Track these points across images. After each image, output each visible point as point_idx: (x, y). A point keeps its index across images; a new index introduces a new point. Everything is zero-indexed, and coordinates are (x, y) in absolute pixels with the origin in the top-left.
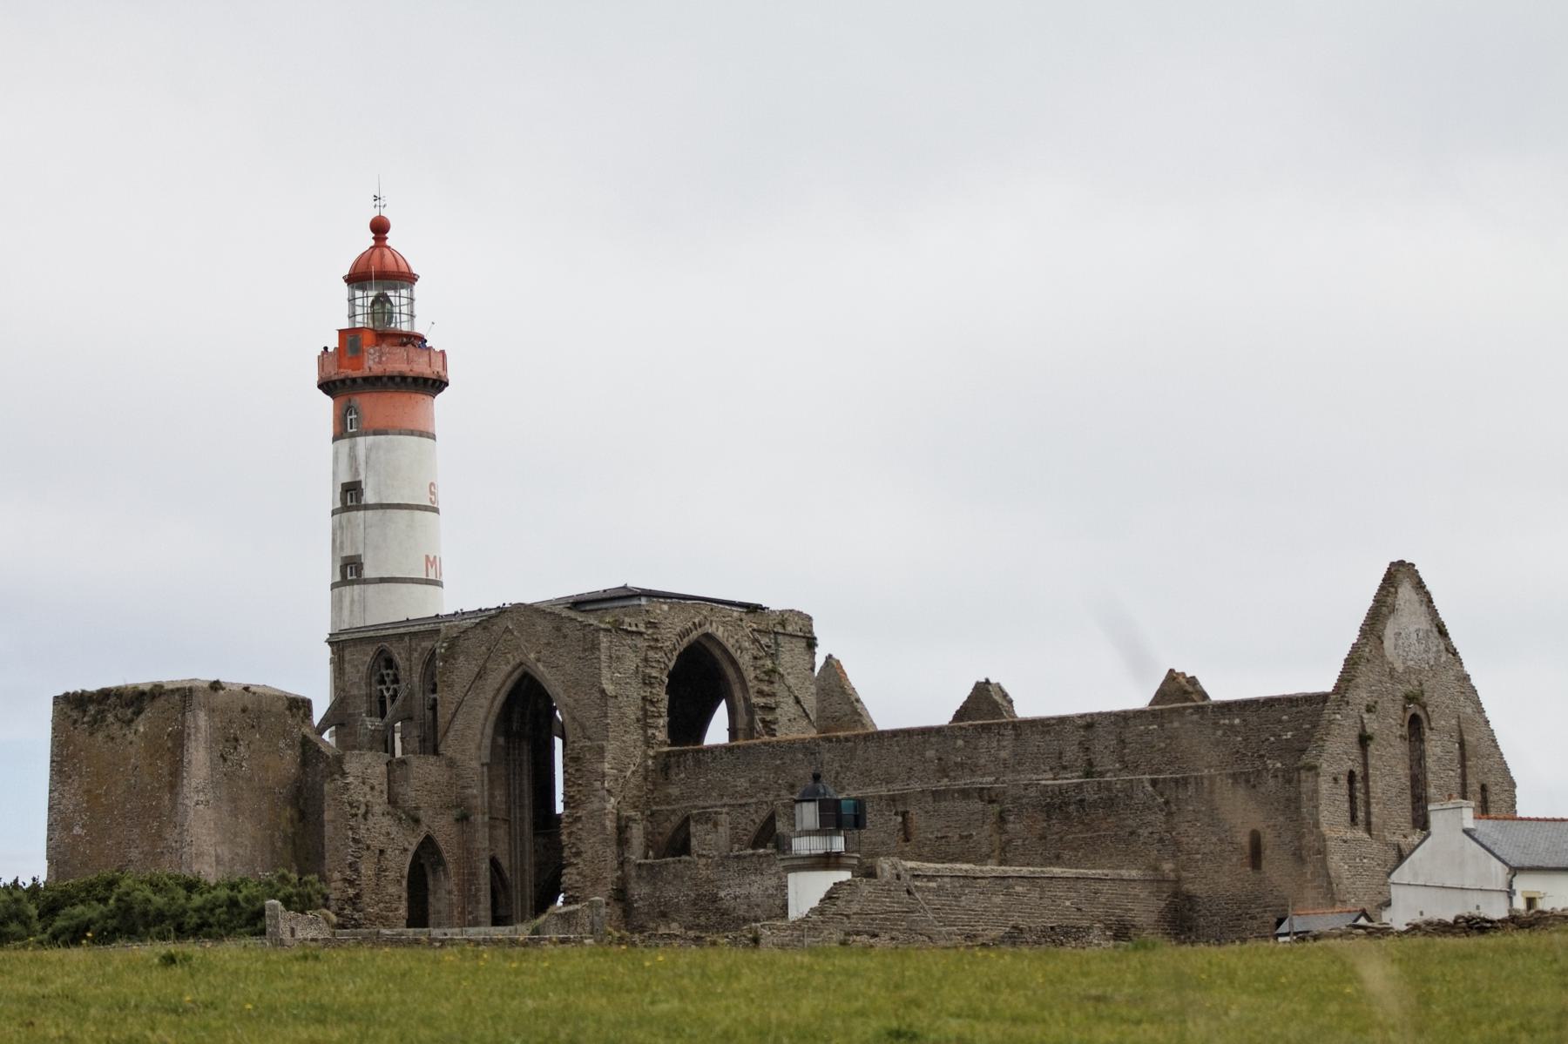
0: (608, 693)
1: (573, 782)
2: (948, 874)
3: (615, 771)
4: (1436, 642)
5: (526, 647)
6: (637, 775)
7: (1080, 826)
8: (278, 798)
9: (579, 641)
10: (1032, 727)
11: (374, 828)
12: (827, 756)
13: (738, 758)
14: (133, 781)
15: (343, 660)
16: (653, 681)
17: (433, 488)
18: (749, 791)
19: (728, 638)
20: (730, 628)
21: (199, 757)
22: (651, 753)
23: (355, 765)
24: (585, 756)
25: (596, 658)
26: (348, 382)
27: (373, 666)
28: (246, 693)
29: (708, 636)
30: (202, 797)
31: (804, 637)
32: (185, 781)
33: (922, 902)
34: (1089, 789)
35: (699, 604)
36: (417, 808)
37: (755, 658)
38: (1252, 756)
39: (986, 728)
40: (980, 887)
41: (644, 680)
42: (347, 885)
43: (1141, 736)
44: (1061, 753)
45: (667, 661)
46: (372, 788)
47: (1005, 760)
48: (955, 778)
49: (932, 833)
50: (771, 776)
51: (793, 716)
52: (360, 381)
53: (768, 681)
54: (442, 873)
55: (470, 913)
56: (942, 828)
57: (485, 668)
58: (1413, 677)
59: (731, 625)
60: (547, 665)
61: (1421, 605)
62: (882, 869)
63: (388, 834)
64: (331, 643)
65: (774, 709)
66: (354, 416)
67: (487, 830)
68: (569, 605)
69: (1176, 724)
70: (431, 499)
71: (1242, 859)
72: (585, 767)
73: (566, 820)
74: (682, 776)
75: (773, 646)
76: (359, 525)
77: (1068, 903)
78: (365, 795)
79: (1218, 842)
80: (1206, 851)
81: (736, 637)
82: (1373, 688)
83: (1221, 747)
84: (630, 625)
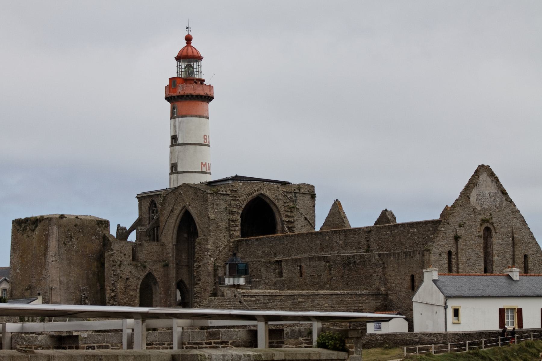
0: (211, 218)
1: (199, 252)
2: (262, 294)
3: (214, 248)
4: (500, 197)
5: (186, 200)
6: (226, 249)
7: (355, 272)
8: (91, 259)
9: (202, 198)
10: (350, 232)
11: (124, 270)
12: (286, 243)
13: (259, 243)
14: (34, 253)
15: (141, 204)
16: (233, 213)
17: (205, 137)
18: (262, 256)
19: (271, 195)
20: (272, 191)
21: (53, 244)
22: (232, 240)
23: (116, 246)
24: (202, 242)
25: (207, 204)
26: (172, 98)
27: (150, 206)
28: (76, 219)
29: (261, 194)
30: (54, 259)
31: (310, 194)
32: (48, 253)
33: (247, 306)
34: (357, 257)
35: (257, 182)
36: (145, 262)
37: (285, 203)
38: (420, 244)
39: (336, 232)
40: (279, 300)
41: (229, 212)
42: (111, 292)
43: (385, 236)
44: (359, 242)
45: (241, 205)
46: (125, 255)
47: (341, 245)
48: (326, 252)
49: (309, 274)
50: (269, 250)
51: (304, 225)
52: (176, 97)
53: (290, 211)
54: (157, 286)
55: (169, 301)
56: (312, 272)
57: (174, 208)
58: (487, 212)
59: (273, 190)
60: (192, 207)
61: (492, 182)
62: (226, 293)
63: (131, 272)
64: (138, 198)
65: (293, 222)
66: (175, 111)
67: (175, 270)
68: (207, 184)
69: (396, 231)
70: (204, 141)
71: (408, 286)
72: (202, 246)
73: (196, 267)
74: (242, 249)
75: (294, 198)
76: (176, 151)
77: (326, 305)
78: (121, 257)
79: (400, 279)
80: (396, 283)
81: (275, 195)
82: (463, 217)
83: (410, 240)
84: (223, 191)
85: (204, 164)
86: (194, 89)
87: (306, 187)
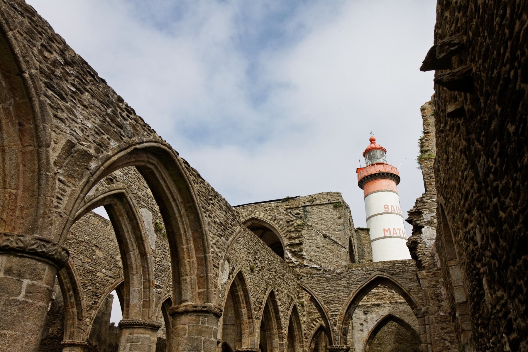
20: (269, 212)
37: (288, 222)
85: (387, 230)
86: (367, 171)
87: (325, 196)
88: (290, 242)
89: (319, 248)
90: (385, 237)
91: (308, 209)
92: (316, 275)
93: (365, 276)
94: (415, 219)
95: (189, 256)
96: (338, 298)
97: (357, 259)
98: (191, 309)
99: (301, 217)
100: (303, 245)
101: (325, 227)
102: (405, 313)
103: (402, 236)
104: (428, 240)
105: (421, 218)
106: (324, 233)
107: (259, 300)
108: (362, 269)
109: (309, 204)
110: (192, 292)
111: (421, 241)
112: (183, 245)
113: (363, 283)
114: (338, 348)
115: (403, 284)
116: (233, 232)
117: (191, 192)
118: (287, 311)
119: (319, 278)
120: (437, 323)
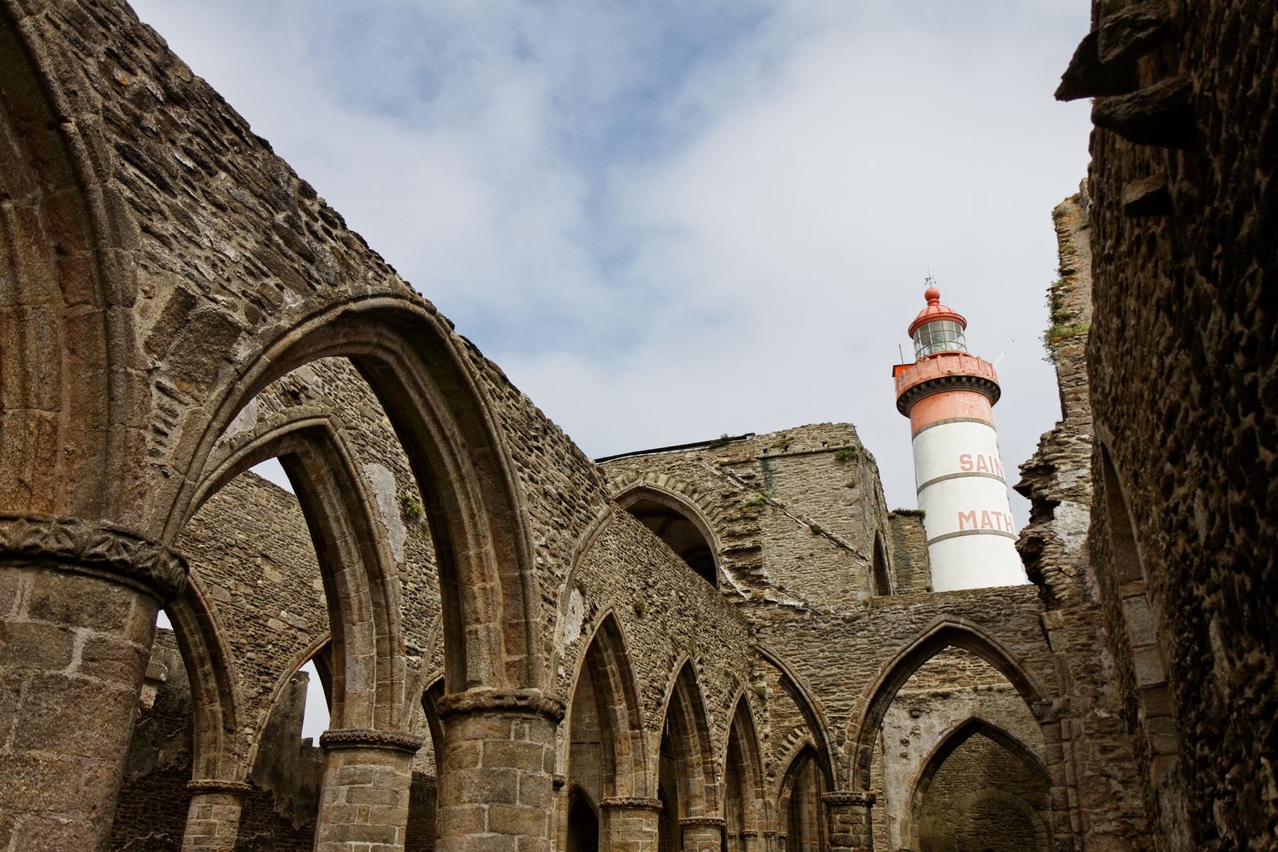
20: (678, 472)
37: (725, 497)
86: (919, 373)
87: (815, 433)
88: (731, 544)
89: (800, 558)
90: (962, 534)
91: (773, 464)
92: (794, 624)
93: (913, 626)
94: (1038, 486)
95: (483, 574)
96: (847, 678)
97: (893, 585)
98: (489, 703)
99: (758, 485)
100: (763, 553)
101: (816, 507)
102: (1010, 714)
103: (1004, 529)
104: (1069, 534)
105: (1054, 482)
106: (814, 522)
107: (655, 684)
108: (905, 609)
109: (776, 452)
110: (492, 663)
111: (1052, 538)
112: (468, 549)
113: (909, 641)
114: (849, 798)
115: (1006, 645)
116: (589, 518)
117: (485, 421)
118: (723, 710)
119: (802, 631)
120: (1091, 736)
